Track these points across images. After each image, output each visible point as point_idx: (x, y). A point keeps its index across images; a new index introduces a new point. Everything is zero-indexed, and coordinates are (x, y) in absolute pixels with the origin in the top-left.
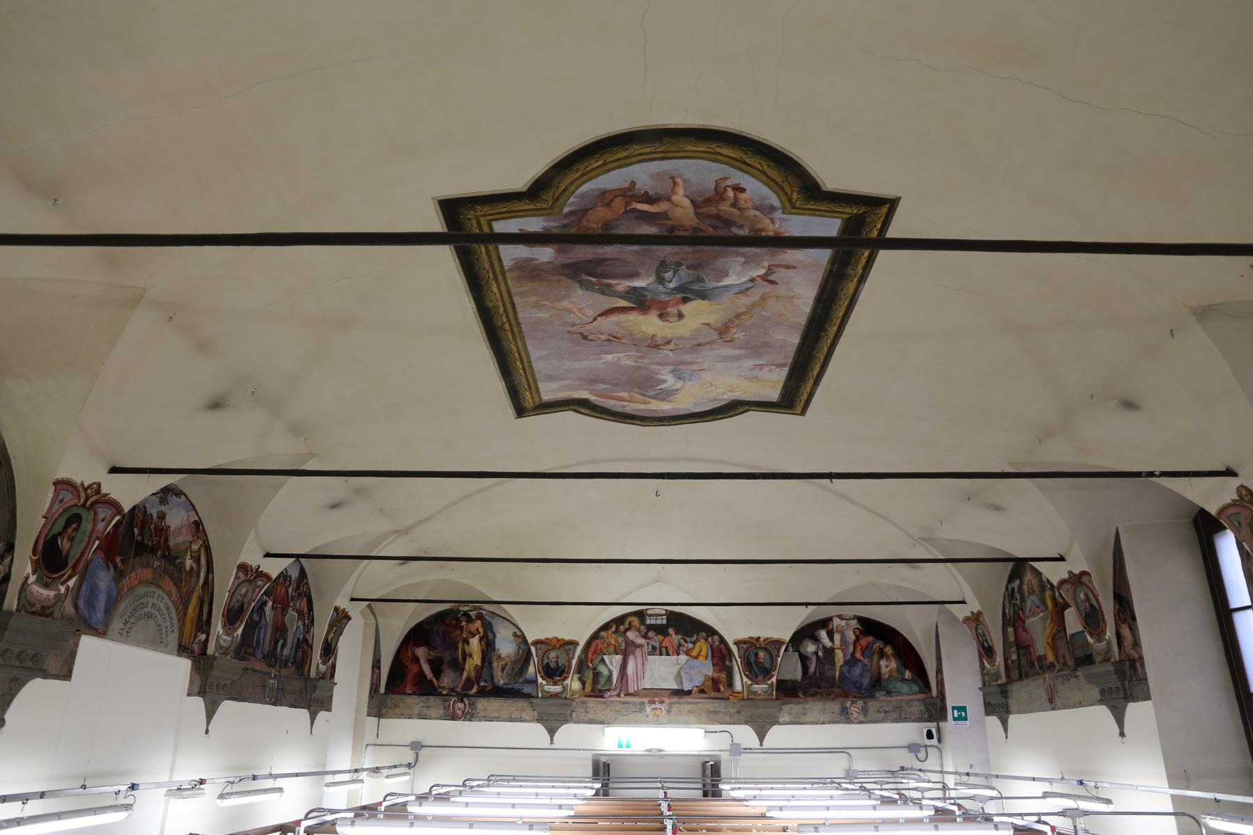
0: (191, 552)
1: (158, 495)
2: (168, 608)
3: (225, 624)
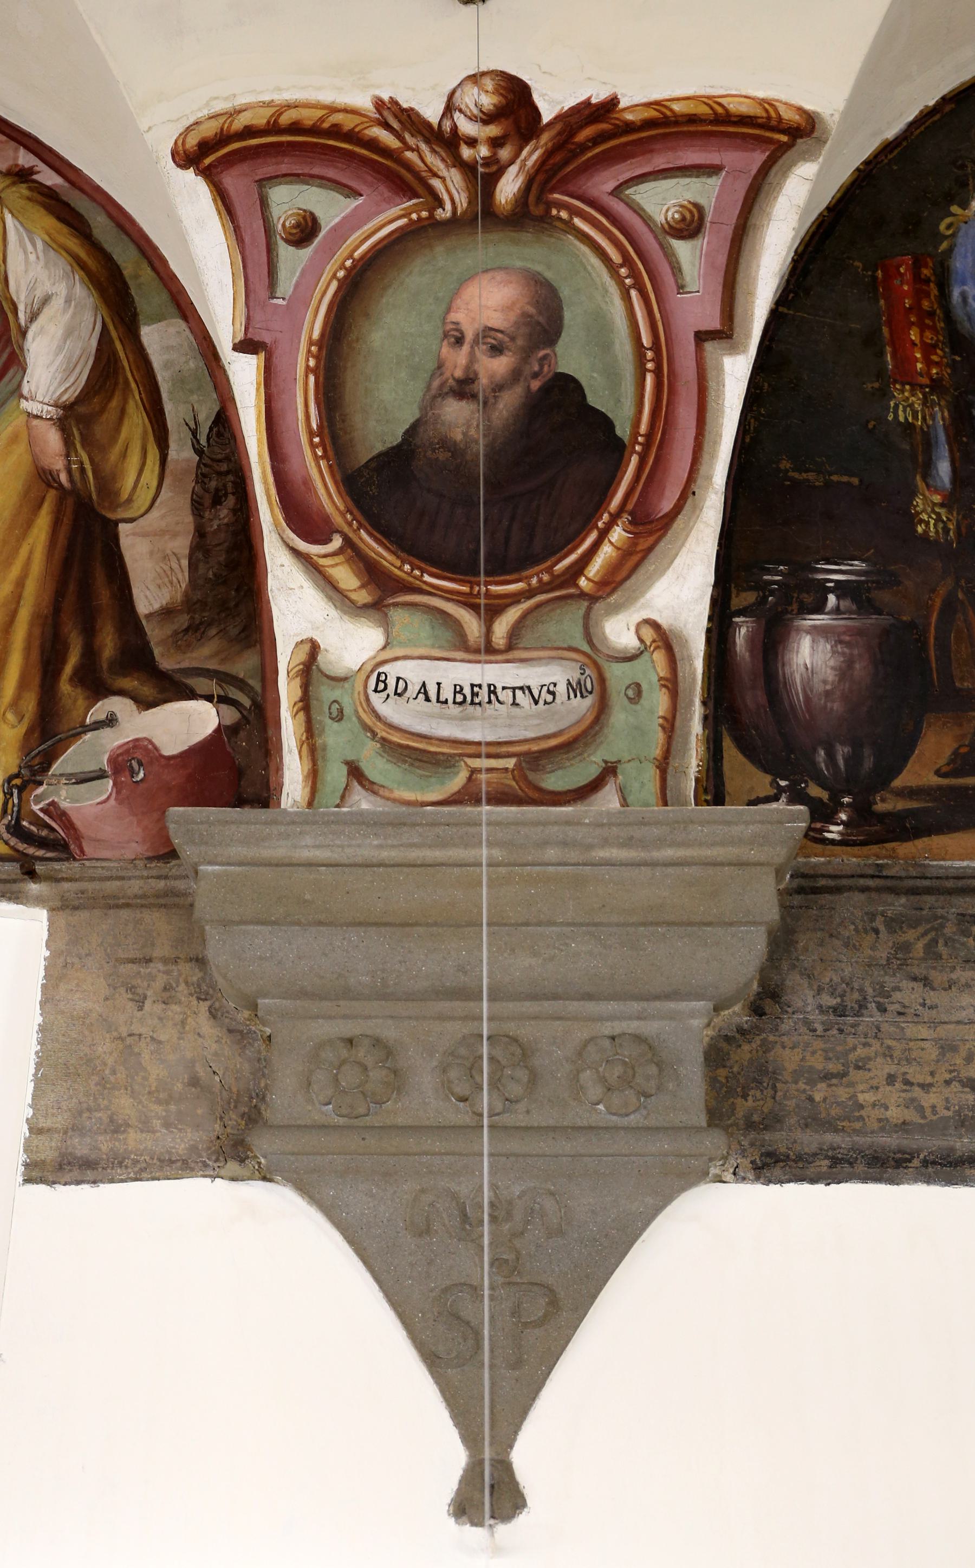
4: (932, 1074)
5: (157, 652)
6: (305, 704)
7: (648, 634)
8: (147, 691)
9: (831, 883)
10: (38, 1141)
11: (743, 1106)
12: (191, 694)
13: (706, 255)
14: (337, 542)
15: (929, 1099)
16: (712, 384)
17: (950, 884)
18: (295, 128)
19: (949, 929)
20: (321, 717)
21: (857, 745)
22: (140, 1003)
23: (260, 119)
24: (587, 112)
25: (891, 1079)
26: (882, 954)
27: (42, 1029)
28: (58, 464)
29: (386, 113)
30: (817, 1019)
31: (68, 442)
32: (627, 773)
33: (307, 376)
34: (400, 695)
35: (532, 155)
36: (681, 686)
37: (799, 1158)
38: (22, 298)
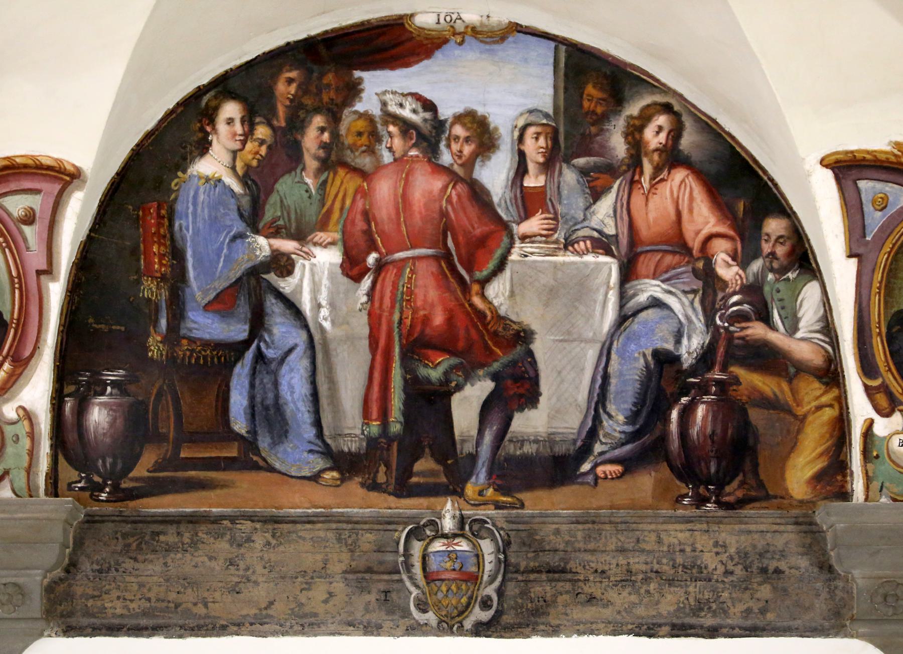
4: (135, 596)
9: (100, 519)
11: (60, 609)
15: (132, 606)
17: (149, 519)
19: (147, 538)
21: (115, 457)
25: (118, 598)
26: (119, 548)
30: (91, 574)
37: (80, 628)
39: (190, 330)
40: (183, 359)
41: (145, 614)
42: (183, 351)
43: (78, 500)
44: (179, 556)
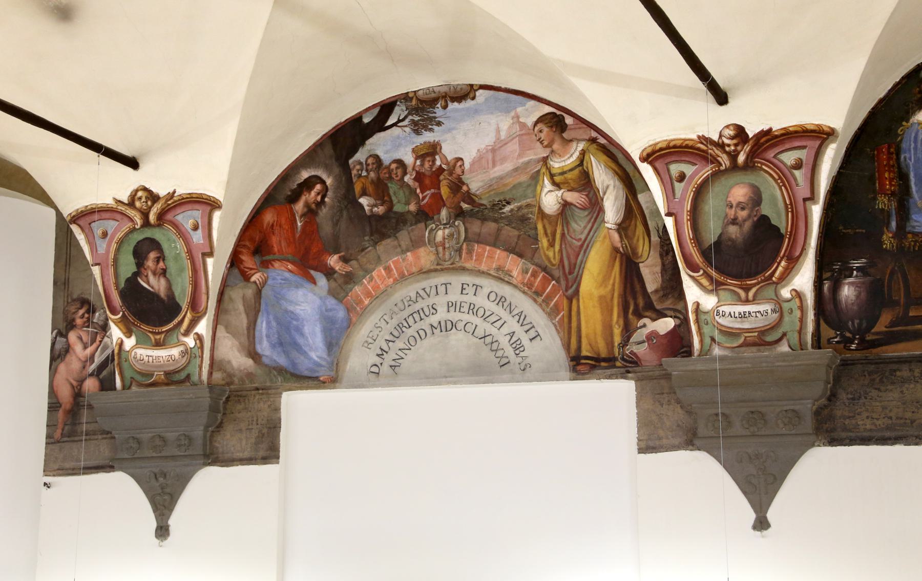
0: (552, 176)
1: (406, 122)
2: (501, 300)
3: (710, 278)
4: (880, 415)
5: (655, 303)
6: (697, 321)
7: (794, 293)
8: (654, 316)
9: (852, 362)
10: (640, 443)
11: (825, 426)
12: (666, 316)
13: (804, 174)
14: (701, 272)
15: (878, 423)
16: (809, 215)
17: (888, 361)
18: (675, 147)
19: (887, 374)
20: (702, 324)
21: (861, 320)
22: (662, 405)
23: (664, 145)
24: (763, 133)
25: (868, 417)
26: (866, 382)
27: (637, 414)
28: (619, 245)
29: (701, 140)
30: (847, 402)
31: (621, 237)
32: (789, 335)
33: (687, 222)
34: (723, 316)
35: (747, 148)
36: (804, 309)
37: (841, 439)
38: (600, 186)
39: (914, 227)
40: (909, 248)
41: (888, 428)
42: (909, 242)
43: (835, 350)
44: (912, 386)
